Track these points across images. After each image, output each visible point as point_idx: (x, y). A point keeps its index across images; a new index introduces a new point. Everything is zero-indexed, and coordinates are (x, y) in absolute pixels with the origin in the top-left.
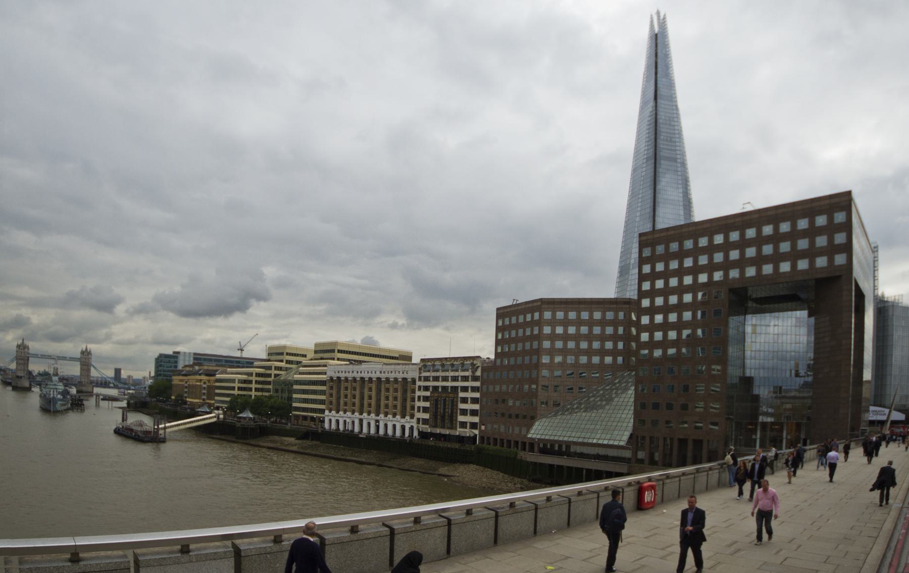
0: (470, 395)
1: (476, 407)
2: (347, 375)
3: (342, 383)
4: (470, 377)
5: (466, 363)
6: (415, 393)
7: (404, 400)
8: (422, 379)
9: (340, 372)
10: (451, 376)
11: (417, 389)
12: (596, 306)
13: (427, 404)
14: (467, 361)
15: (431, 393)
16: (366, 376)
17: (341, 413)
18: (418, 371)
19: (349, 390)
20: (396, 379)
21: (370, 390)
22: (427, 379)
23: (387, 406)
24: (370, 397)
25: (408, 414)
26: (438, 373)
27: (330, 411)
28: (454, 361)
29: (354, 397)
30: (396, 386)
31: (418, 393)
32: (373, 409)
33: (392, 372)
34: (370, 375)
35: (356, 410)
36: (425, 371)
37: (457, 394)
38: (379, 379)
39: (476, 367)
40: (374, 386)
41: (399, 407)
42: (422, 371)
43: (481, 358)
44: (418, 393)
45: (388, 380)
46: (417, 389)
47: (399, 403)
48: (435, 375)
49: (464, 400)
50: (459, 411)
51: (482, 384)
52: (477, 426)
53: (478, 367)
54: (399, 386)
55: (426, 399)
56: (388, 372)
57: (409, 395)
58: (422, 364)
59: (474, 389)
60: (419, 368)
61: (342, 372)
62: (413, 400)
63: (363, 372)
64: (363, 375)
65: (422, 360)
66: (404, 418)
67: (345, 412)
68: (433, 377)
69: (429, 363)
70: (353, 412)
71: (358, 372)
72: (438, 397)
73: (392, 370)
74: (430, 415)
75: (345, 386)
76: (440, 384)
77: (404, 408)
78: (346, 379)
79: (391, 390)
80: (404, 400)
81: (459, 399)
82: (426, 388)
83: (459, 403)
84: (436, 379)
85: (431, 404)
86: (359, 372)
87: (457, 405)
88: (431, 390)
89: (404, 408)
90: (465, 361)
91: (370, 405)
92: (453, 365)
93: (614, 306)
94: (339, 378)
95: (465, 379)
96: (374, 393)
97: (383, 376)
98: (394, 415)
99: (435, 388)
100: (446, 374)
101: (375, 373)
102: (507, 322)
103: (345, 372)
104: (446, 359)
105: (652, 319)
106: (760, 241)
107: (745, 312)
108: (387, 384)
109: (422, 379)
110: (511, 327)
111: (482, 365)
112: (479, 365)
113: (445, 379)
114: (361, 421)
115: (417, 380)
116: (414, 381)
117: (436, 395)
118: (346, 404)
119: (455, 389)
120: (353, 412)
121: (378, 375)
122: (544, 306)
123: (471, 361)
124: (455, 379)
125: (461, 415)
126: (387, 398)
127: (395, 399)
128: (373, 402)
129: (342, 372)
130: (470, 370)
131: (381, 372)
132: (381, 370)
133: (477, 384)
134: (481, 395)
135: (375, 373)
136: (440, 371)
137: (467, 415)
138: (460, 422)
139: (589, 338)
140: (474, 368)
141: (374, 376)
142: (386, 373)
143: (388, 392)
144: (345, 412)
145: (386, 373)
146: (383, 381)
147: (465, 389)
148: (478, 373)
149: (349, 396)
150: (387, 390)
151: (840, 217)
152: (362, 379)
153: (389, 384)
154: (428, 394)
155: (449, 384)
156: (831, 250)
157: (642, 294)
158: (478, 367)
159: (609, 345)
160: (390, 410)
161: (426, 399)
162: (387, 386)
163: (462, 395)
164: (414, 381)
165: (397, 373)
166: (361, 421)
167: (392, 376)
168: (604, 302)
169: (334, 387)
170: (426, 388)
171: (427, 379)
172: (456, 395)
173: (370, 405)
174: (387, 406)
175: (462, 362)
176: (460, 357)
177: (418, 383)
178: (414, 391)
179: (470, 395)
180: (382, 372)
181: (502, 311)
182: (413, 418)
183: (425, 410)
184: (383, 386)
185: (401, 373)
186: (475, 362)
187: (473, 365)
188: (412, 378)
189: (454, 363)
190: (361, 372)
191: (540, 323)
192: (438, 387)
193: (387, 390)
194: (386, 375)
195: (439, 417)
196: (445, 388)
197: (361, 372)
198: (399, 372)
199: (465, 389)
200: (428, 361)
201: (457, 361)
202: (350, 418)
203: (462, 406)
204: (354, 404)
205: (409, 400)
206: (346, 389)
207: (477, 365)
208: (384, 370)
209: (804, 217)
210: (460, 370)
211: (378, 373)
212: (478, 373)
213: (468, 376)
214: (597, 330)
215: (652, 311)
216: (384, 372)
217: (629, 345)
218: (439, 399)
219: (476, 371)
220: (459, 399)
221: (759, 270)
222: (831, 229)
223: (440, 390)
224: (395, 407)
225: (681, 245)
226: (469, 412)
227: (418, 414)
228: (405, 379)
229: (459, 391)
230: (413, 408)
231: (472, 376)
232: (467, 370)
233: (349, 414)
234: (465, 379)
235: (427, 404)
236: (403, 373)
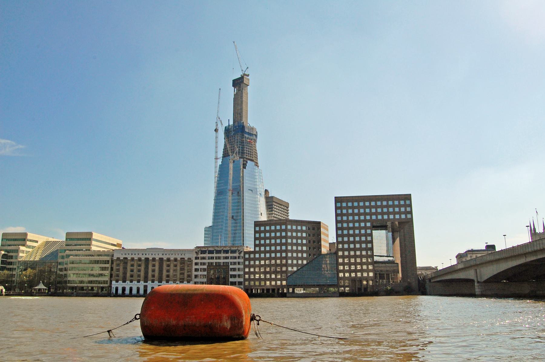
0: (237, 266)
2: (133, 256)
3: (129, 262)
9: (127, 254)
17: (128, 282)
18: (195, 253)
19: (135, 266)
20: (176, 260)
21: (154, 266)
22: (204, 258)
23: (168, 276)
24: (153, 271)
25: (185, 279)
26: (213, 255)
27: (117, 281)
29: (139, 271)
30: (175, 263)
31: (194, 267)
34: (154, 256)
35: (141, 280)
38: (161, 259)
39: (240, 252)
40: (157, 264)
44: (194, 267)
52: (242, 284)
53: (242, 252)
58: (199, 249)
60: (196, 252)
61: (129, 254)
62: (190, 271)
63: (147, 255)
64: (147, 256)
67: (131, 281)
70: (139, 281)
71: (143, 254)
75: (131, 264)
76: (214, 261)
78: (133, 259)
79: (172, 265)
81: (230, 269)
82: (204, 264)
86: (144, 255)
87: (229, 273)
88: (207, 265)
91: (153, 276)
94: (126, 258)
96: (157, 268)
99: (210, 264)
103: (132, 254)
114: (146, 287)
115: (193, 259)
118: (132, 276)
119: (227, 265)
120: (139, 281)
121: (161, 256)
124: (226, 258)
126: (168, 271)
128: (157, 274)
129: (129, 254)
130: (237, 253)
138: (230, 282)
142: (168, 255)
143: (169, 267)
144: (131, 281)
145: (168, 255)
148: (242, 255)
149: (135, 271)
150: (168, 266)
152: (147, 260)
153: (169, 262)
154: (205, 267)
155: (222, 261)
158: (242, 252)
162: (168, 263)
163: (231, 267)
165: (177, 255)
166: (146, 287)
169: (121, 264)
170: (204, 264)
171: (204, 258)
172: (227, 267)
173: (153, 276)
177: (195, 261)
179: (237, 266)
186: (239, 249)
187: (239, 251)
189: (224, 249)
190: (146, 254)
193: (168, 266)
194: (168, 256)
196: (218, 264)
197: (146, 254)
201: (226, 248)
202: (136, 285)
204: (139, 276)
206: (132, 265)
207: (241, 251)
212: (242, 255)
219: (241, 253)
226: (237, 276)
229: (230, 264)
230: (189, 276)
233: (135, 282)
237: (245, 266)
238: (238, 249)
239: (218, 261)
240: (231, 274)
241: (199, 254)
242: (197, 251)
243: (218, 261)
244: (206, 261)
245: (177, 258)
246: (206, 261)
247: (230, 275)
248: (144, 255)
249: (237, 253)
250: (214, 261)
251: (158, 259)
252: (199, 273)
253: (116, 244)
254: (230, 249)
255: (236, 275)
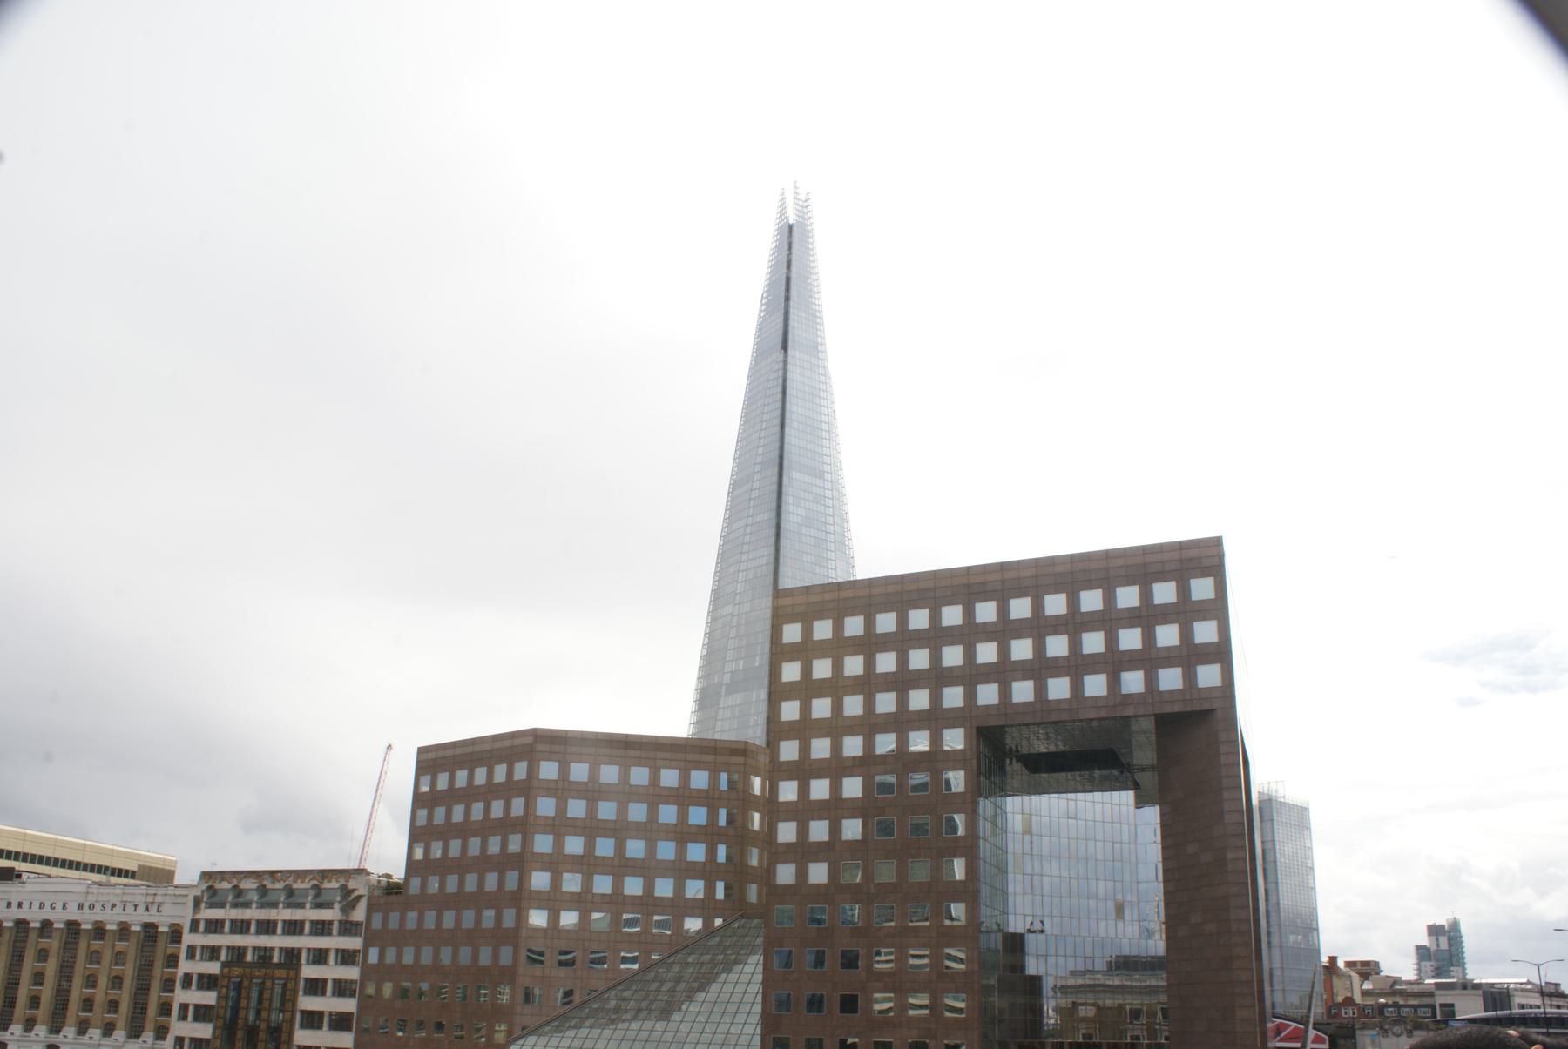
0: (332, 972)
1: (349, 1005)
4: (336, 926)
5: (326, 885)
6: (176, 966)
7: (143, 989)
8: (202, 927)
10: (284, 921)
11: (183, 955)
12: (668, 755)
13: (209, 998)
14: (330, 881)
15: (224, 965)
16: (35, 917)
18: (191, 904)
20: (124, 929)
22: (215, 926)
23: (88, 1004)
24: (39, 978)
25: (150, 1025)
26: (248, 911)
28: (295, 882)
31: (185, 967)
32: (43, 1012)
33: (113, 906)
34: (47, 914)
36: (211, 906)
37: (297, 967)
38: (73, 926)
40: (54, 944)
41: (124, 1007)
42: (203, 905)
43: (369, 874)
44: (185, 967)
45: (99, 931)
46: (183, 955)
47: (125, 997)
48: (240, 917)
49: (316, 987)
50: (298, 1017)
51: (367, 945)
53: (360, 897)
54: (130, 947)
55: (207, 982)
56: (103, 906)
57: (158, 970)
58: (204, 886)
59: (347, 957)
63: (26, 905)
64: (23, 914)
65: (206, 875)
66: (138, 1036)
68: (232, 921)
69: (226, 885)
72: (242, 976)
73: (113, 900)
74: (214, 1033)
76: (250, 941)
77: (139, 1009)
79: (107, 958)
80: (143, 989)
81: (302, 983)
82: (212, 953)
83: (301, 993)
84: (241, 927)
85: (219, 997)
86: (15, 905)
87: (294, 1002)
88: (223, 957)
89: (139, 1009)
90: (326, 881)
91: (35, 1001)
92: (290, 892)
93: (710, 758)
95: (322, 928)
96: (51, 967)
97: (87, 920)
98: (108, 1029)
99: (238, 953)
100: (271, 914)
101: (64, 906)
102: (443, 782)
104: (272, 873)
105: (804, 790)
106: (1039, 627)
107: (1003, 791)
108: (95, 939)
109: (202, 927)
110: (452, 796)
111: (369, 892)
112: (362, 890)
113: (267, 927)
116: (176, 934)
117: (236, 971)
119: (292, 955)
121: (73, 914)
122: (540, 747)
123: (342, 881)
124: (294, 928)
125: (302, 1027)
126: (91, 981)
127: (117, 981)
128: (47, 993)
130: (337, 906)
131: (81, 907)
132: (81, 900)
133: (354, 943)
134: (363, 973)
135: (64, 906)
136: (254, 905)
137: (320, 1028)
139: (650, 831)
140: (349, 900)
141: (59, 918)
142: (98, 907)
146: (86, 930)
147: (320, 957)
148: (359, 914)
150: (94, 957)
151: (1202, 589)
153: (102, 939)
154: (213, 968)
155: (278, 941)
156: (1190, 656)
157: (776, 731)
158: (360, 897)
159: (696, 852)
160: (99, 1014)
161: (207, 982)
162: (96, 944)
163: (309, 971)
164: (176, 934)
165: (130, 908)
167: (112, 920)
168: (685, 746)
171: (215, 926)
172: (292, 973)
173: (35, 1001)
174: (88, 1004)
175: (315, 882)
176: (312, 871)
177: (188, 939)
178: (173, 961)
180: (86, 907)
181: (431, 756)
182: (164, 1038)
183: (202, 1013)
184: (83, 945)
185: (141, 908)
186: (352, 885)
187: (346, 892)
188: (172, 925)
189: (295, 886)
190: (20, 905)
191: (528, 789)
192: (245, 948)
194: (98, 915)
195: (240, 1034)
197: (20, 905)
198: (136, 906)
199: (320, 957)
200: (223, 879)
201: (302, 882)
203: (308, 1003)
205: (156, 986)
207: (356, 894)
208: (91, 899)
209: (1129, 582)
210: (308, 906)
211: (72, 907)
212: (359, 914)
213: (331, 923)
214: (668, 814)
215: (804, 771)
216: (92, 907)
217: (744, 854)
218: (246, 983)
220: (302, 983)
221: (1041, 690)
222: (1185, 612)
223: (249, 958)
224: (114, 1006)
225: (870, 624)
227: (182, 1024)
228: (150, 929)
230: (166, 1009)
231: (340, 922)
232: (329, 905)
234: (322, 928)
235: (209, 998)
236: (147, 909)
237: (367, 971)
238: (344, 887)
239: (265, 941)
240: (303, 1008)
241: (200, 909)
242: (199, 893)
243: (265, 941)
244: (225, 940)
245: (130, 925)
246: (225, 940)
247: (303, 1012)
248: (15, 905)
249: (337, 906)
250: (250, 941)
251: (61, 926)
252: (196, 997)
253: (135, 869)
254: (315, 887)
255: (321, 1014)
